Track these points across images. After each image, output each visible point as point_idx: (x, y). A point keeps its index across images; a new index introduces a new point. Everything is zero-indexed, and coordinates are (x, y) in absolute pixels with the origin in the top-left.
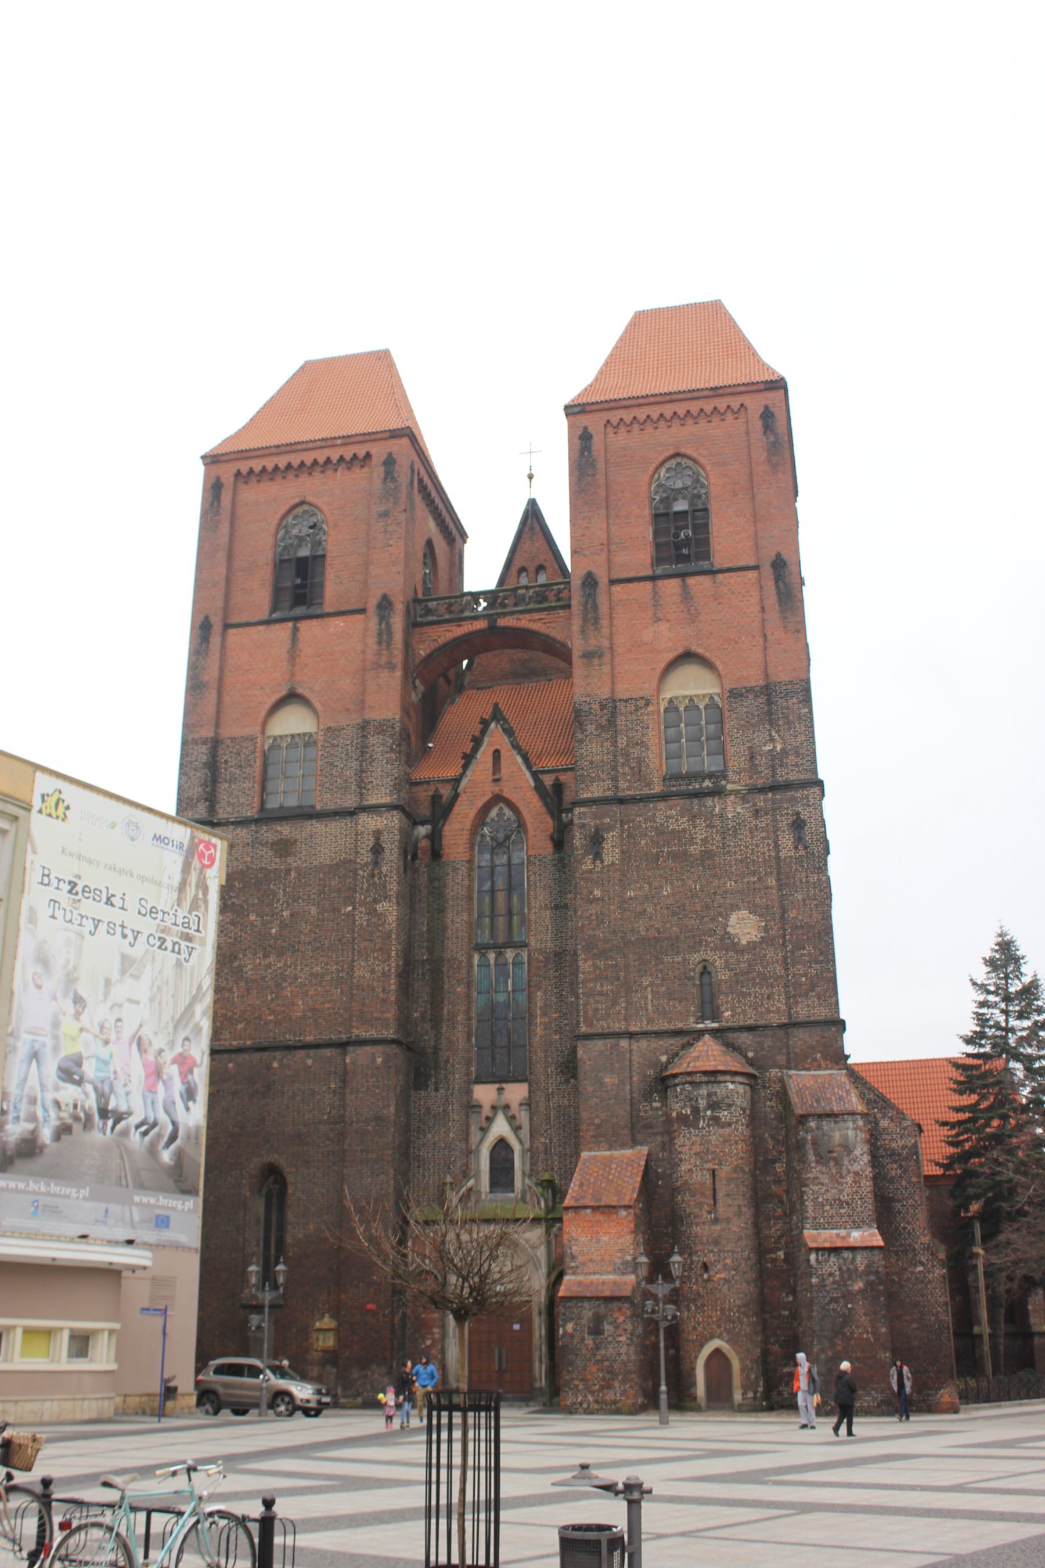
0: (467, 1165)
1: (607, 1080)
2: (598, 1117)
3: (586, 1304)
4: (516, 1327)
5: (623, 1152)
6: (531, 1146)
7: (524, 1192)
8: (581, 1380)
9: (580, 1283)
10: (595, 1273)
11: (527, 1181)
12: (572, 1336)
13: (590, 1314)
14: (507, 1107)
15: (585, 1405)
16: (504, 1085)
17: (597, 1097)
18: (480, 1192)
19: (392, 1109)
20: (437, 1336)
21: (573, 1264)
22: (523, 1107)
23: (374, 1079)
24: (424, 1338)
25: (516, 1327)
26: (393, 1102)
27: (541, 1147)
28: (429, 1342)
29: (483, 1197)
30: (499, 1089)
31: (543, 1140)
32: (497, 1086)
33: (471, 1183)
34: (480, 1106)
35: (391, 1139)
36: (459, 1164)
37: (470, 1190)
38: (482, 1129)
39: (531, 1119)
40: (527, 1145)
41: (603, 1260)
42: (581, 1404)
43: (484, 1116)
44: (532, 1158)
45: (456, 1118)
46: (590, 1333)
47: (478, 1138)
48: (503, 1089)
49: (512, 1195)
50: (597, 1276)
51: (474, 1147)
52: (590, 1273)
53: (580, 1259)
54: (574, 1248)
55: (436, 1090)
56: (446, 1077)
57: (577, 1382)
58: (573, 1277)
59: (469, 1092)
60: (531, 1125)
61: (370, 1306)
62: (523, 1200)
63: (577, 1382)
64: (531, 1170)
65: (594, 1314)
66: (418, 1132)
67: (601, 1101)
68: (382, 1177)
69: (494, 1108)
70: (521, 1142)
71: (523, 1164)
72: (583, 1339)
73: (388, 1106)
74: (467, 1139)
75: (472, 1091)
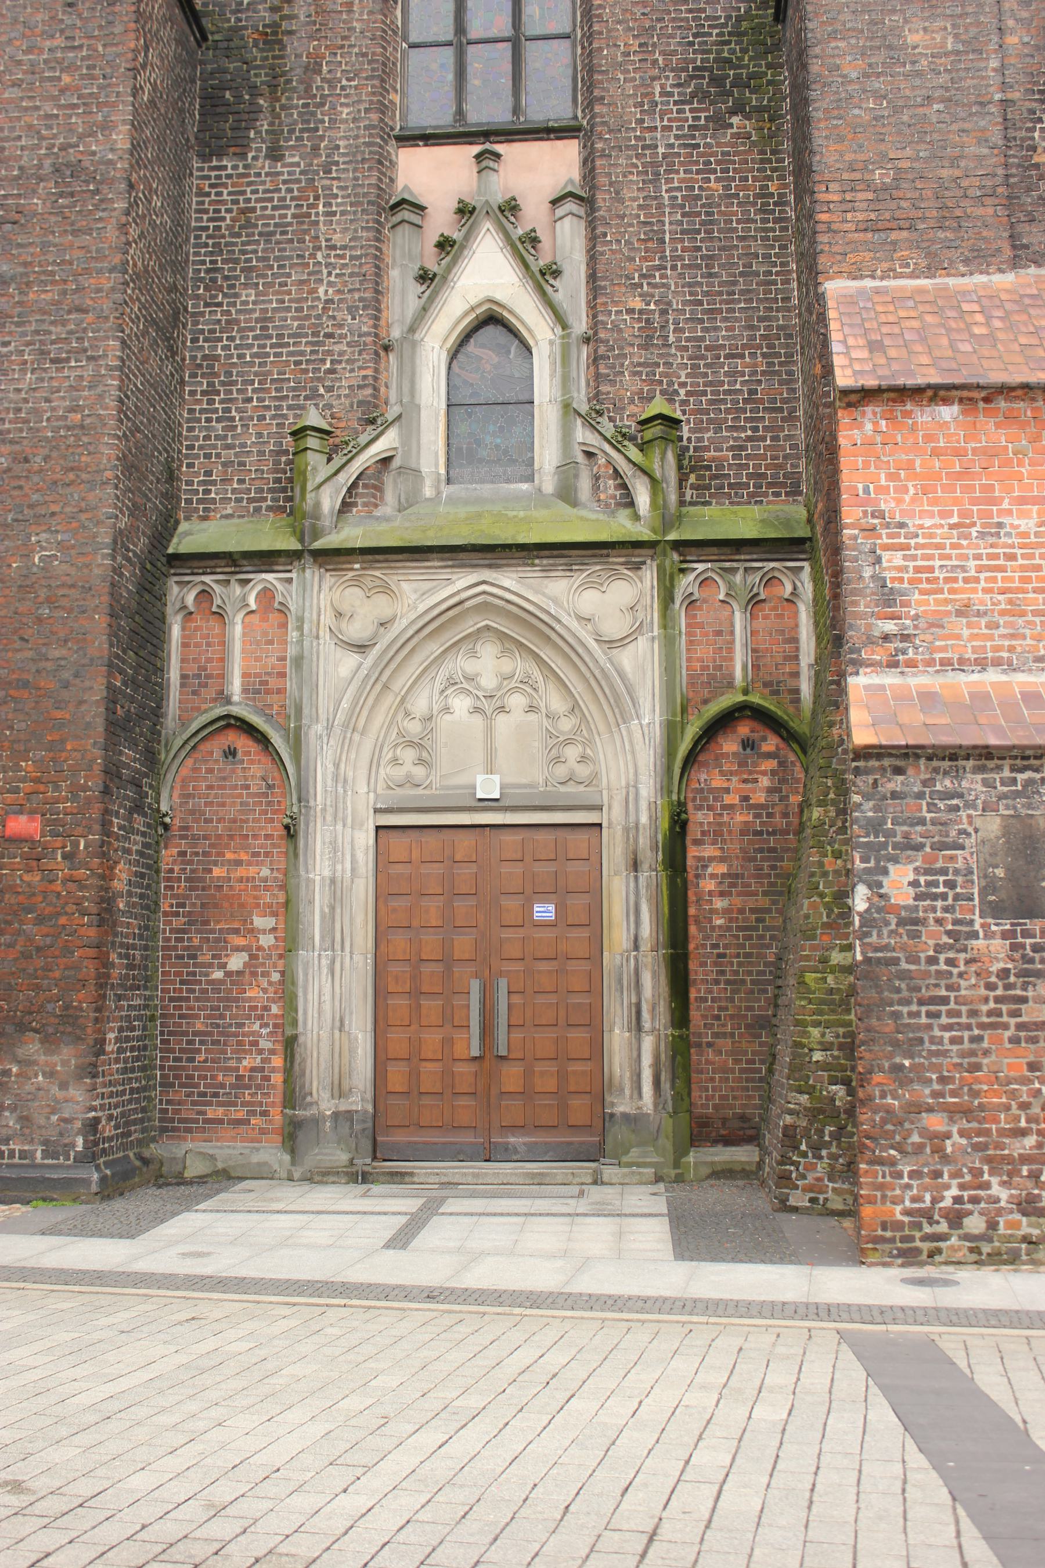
0: (375, 383)
1: (912, 39)
2: (883, 159)
3: (973, 784)
4: (544, 911)
5: (980, 279)
6: (595, 324)
7: (567, 471)
8: (953, 1112)
9: (928, 698)
10: (982, 664)
11: (582, 434)
12: (911, 922)
13: (992, 826)
14: (511, 208)
15: (975, 1224)
16: (499, 148)
17: (879, 97)
18: (417, 471)
19: (121, 138)
20: (266, 941)
21: (890, 627)
22: (570, 206)
23: (59, 41)
24: (220, 948)
25: (544, 911)
26: (123, 113)
27: (631, 328)
28: (236, 962)
29: (428, 492)
30: (479, 157)
31: (637, 304)
32: (476, 149)
33: (387, 442)
34: (420, 208)
35: (112, 234)
36: (347, 379)
37: (386, 461)
38: (425, 277)
39: (593, 239)
40: (580, 325)
41: (1015, 611)
42: (956, 1219)
43: (432, 237)
44: (595, 360)
45: (337, 239)
46: (995, 910)
47: (413, 304)
48: (497, 156)
49: (525, 486)
50: (993, 676)
51: (396, 333)
52: (962, 665)
53: (919, 604)
54: (892, 559)
55: (275, 154)
56: (307, 115)
57: (936, 1122)
58: (890, 679)
59: (384, 165)
60: (592, 258)
61: (21, 824)
62: (567, 494)
63: (936, 1122)
64: (596, 397)
65: (1006, 831)
66: (212, 285)
67: (897, 110)
68: (78, 369)
69: (465, 211)
70: (560, 319)
71: (566, 381)
72: (962, 935)
73: (107, 127)
74: (375, 305)
75: (393, 164)
